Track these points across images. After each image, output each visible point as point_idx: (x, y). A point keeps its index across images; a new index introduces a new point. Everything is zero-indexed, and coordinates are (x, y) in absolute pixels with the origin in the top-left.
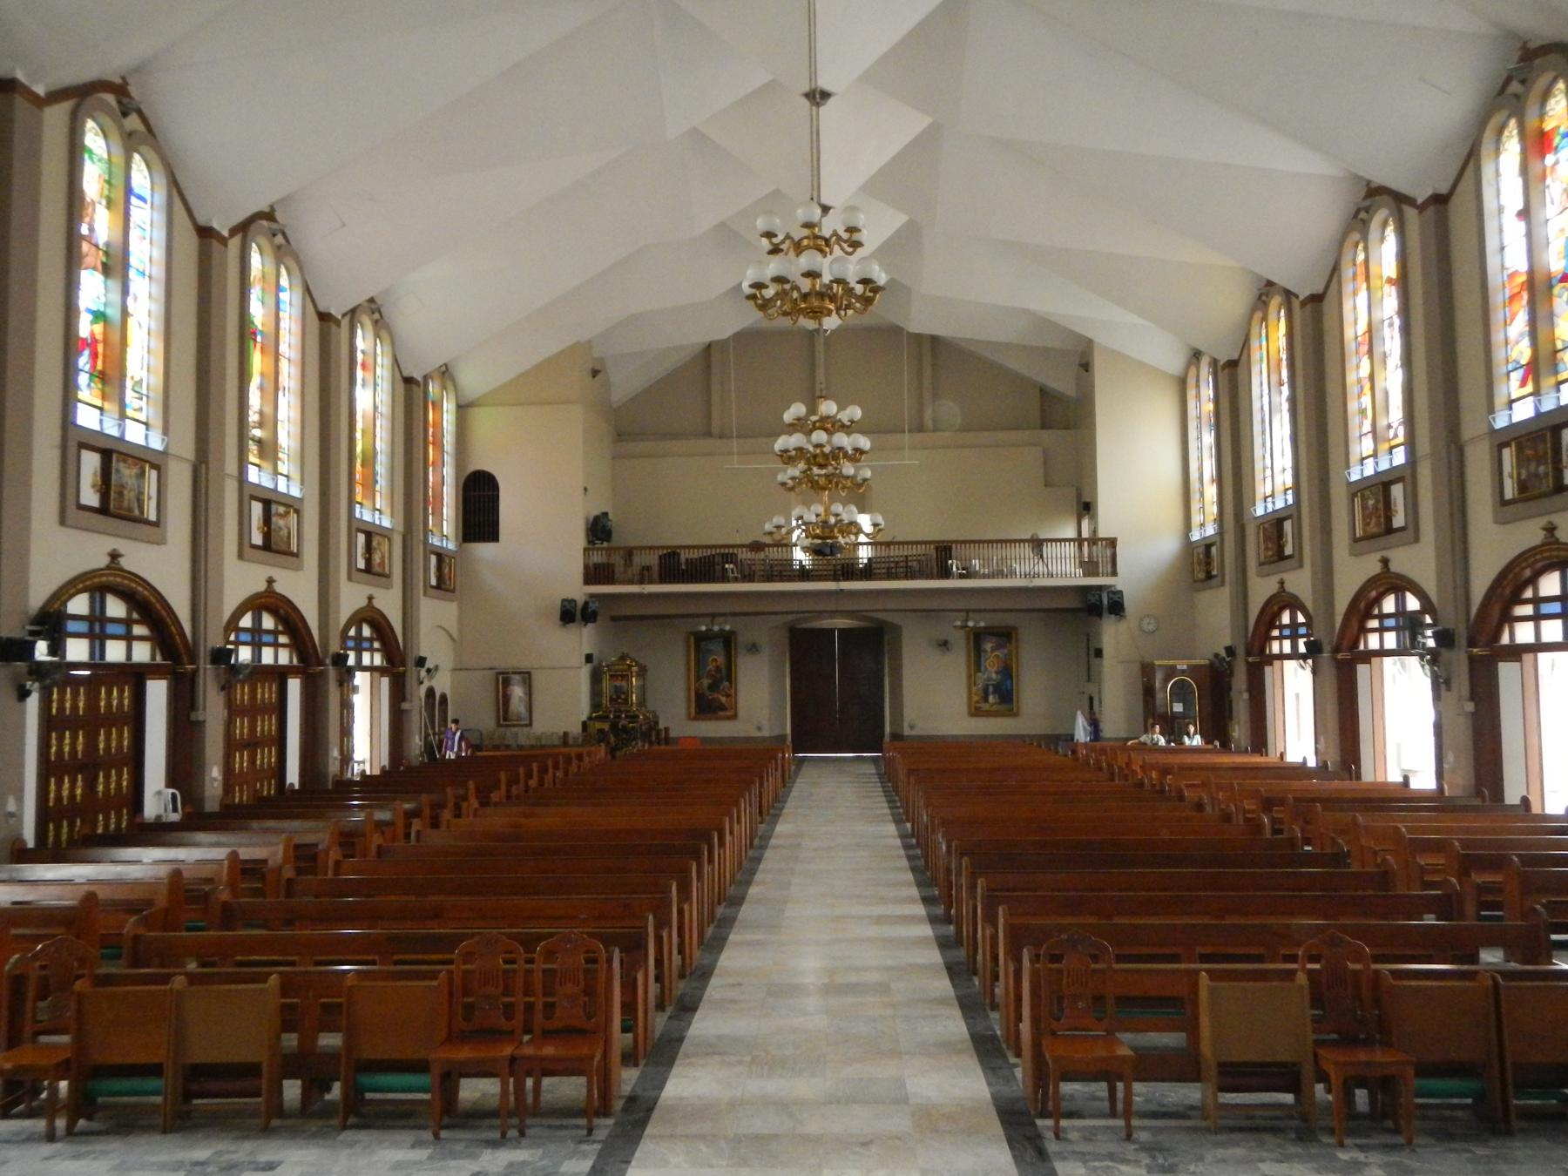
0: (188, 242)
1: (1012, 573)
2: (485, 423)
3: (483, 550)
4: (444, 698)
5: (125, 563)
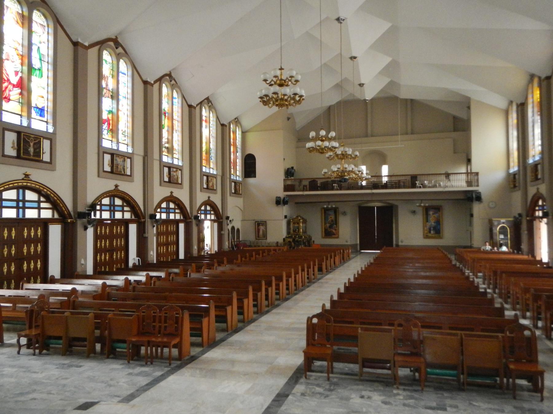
0: (140, 86)
1: (440, 185)
2: (251, 137)
3: (251, 180)
4: (238, 230)
5: (120, 188)
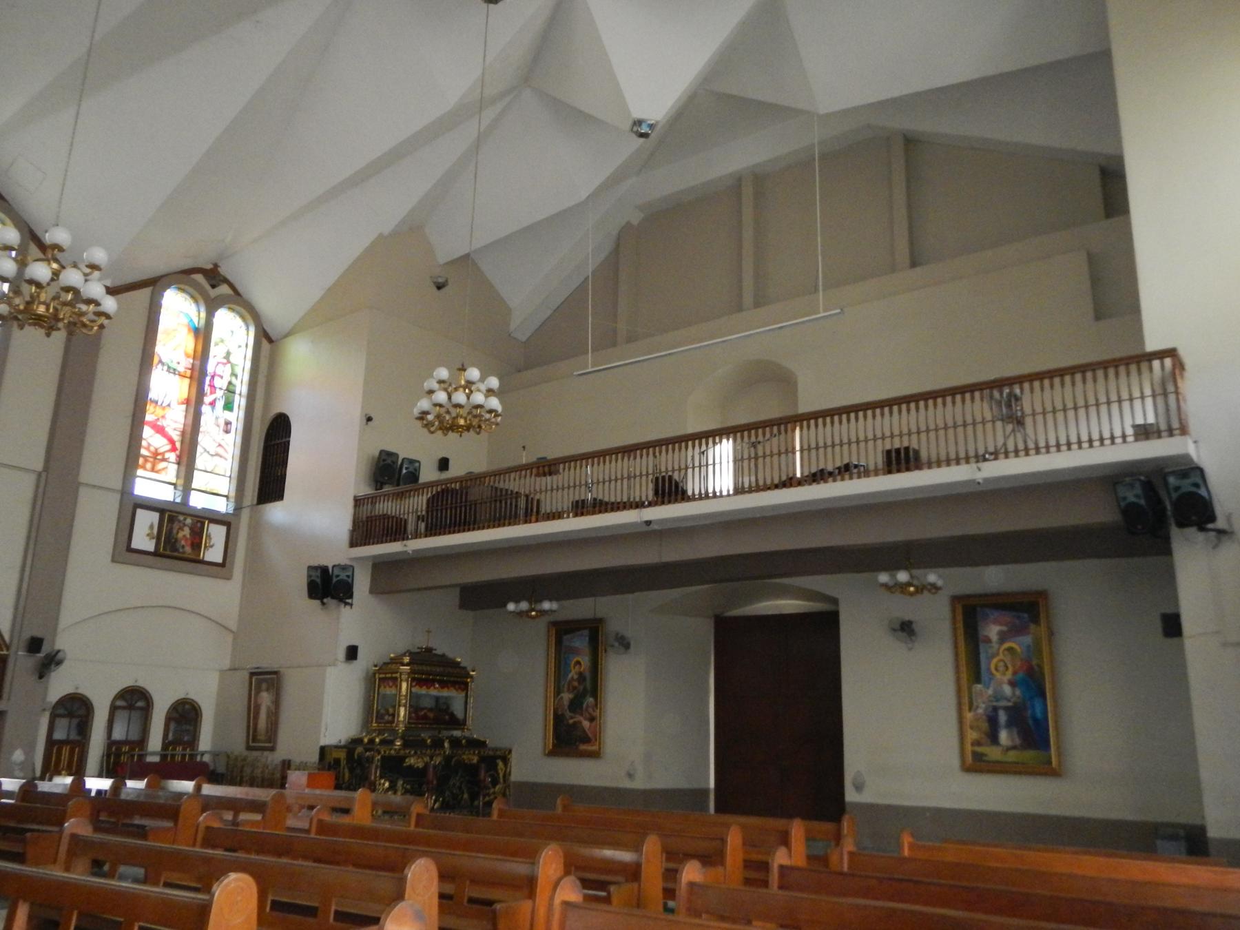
2: (302, 359)
3: (276, 513)
